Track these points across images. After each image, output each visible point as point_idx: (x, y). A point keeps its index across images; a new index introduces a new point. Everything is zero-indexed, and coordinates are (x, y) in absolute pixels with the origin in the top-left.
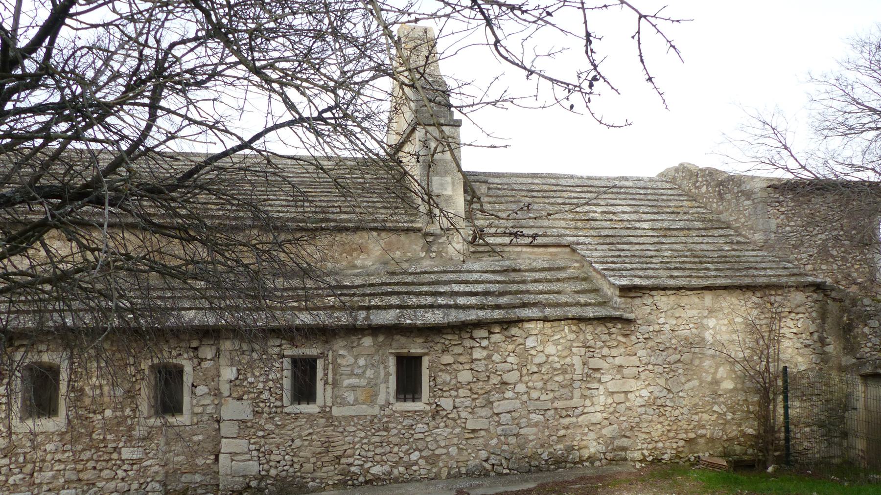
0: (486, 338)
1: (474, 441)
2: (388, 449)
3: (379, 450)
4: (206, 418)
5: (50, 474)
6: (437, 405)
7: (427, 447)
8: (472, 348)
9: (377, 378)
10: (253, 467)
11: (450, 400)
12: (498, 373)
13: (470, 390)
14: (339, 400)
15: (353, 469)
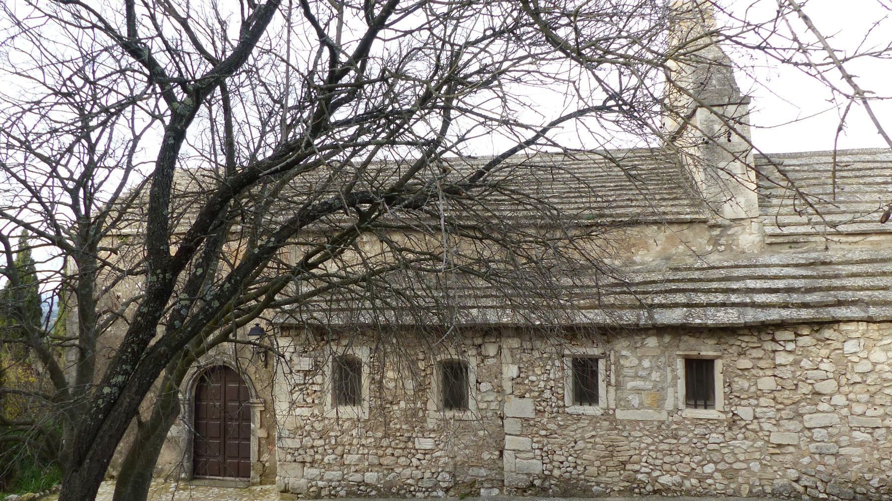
0: (792, 341)
1: (781, 458)
2: (678, 458)
3: (668, 459)
4: (490, 414)
5: (357, 457)
6: (734, 414)
7: (723, 460)
8: (774, 351)
9: (664, 380)
10: (537, 466)
11: (749, 410)
12: (809, 381)
13: (774, 399)
14: (622, 403)
15: (640, 476)
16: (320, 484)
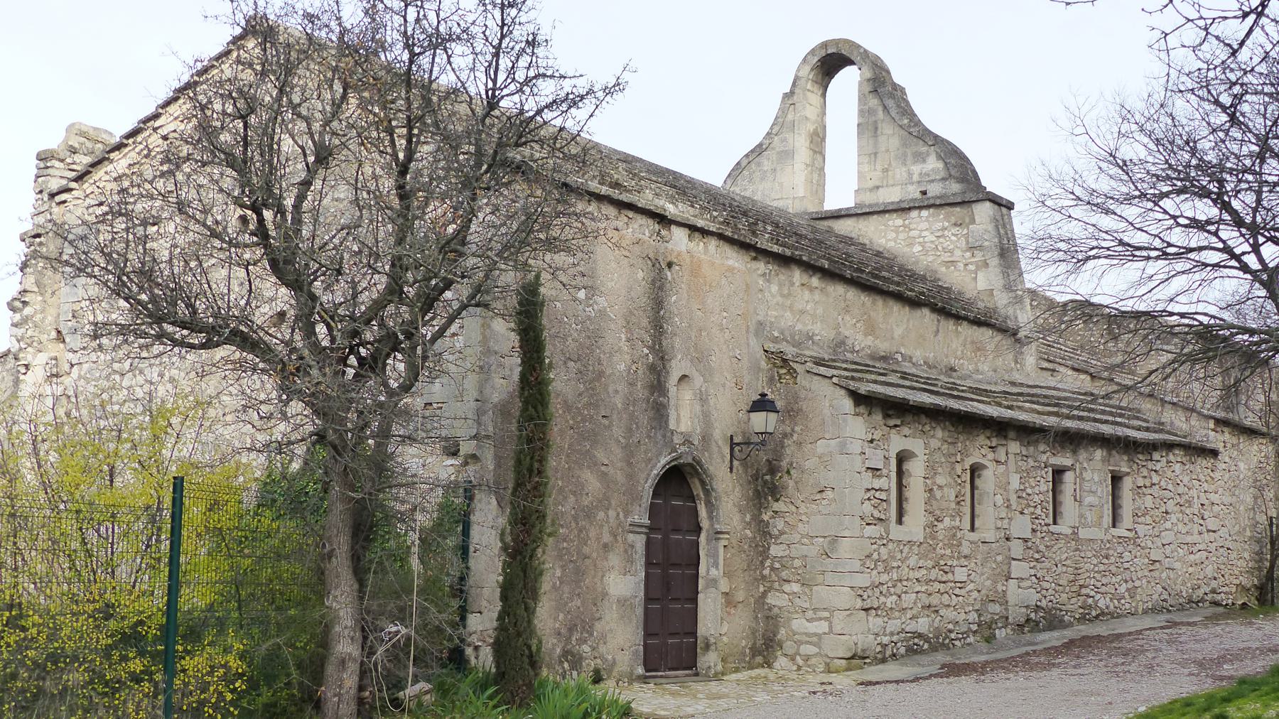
10: (1033, 597)
16: (886, 640)
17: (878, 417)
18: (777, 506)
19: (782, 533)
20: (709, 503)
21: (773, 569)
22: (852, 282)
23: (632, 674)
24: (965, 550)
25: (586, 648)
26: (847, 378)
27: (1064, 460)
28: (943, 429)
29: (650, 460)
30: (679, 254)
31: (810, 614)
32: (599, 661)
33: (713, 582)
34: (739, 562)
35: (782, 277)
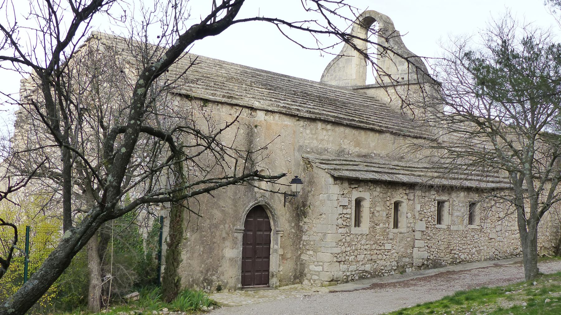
10: (426, 255)
16: (348, 274)
17: (346, 185)
18: (305, 220)
19: (307, 231)
20: (273, 219)
21: (303, 245)
22: (347, 126)
23: (235, 287)
24: (391, 236)
25: (214, 277)
26: (332, 169)
27: (444, 198)
28: (380, 188)
29: (245, 204)
30: (261, 122)
31: (316, 263)
32: (220, 282)
33: (276, 251)
34: (289, 242)
35: (312, 127)
